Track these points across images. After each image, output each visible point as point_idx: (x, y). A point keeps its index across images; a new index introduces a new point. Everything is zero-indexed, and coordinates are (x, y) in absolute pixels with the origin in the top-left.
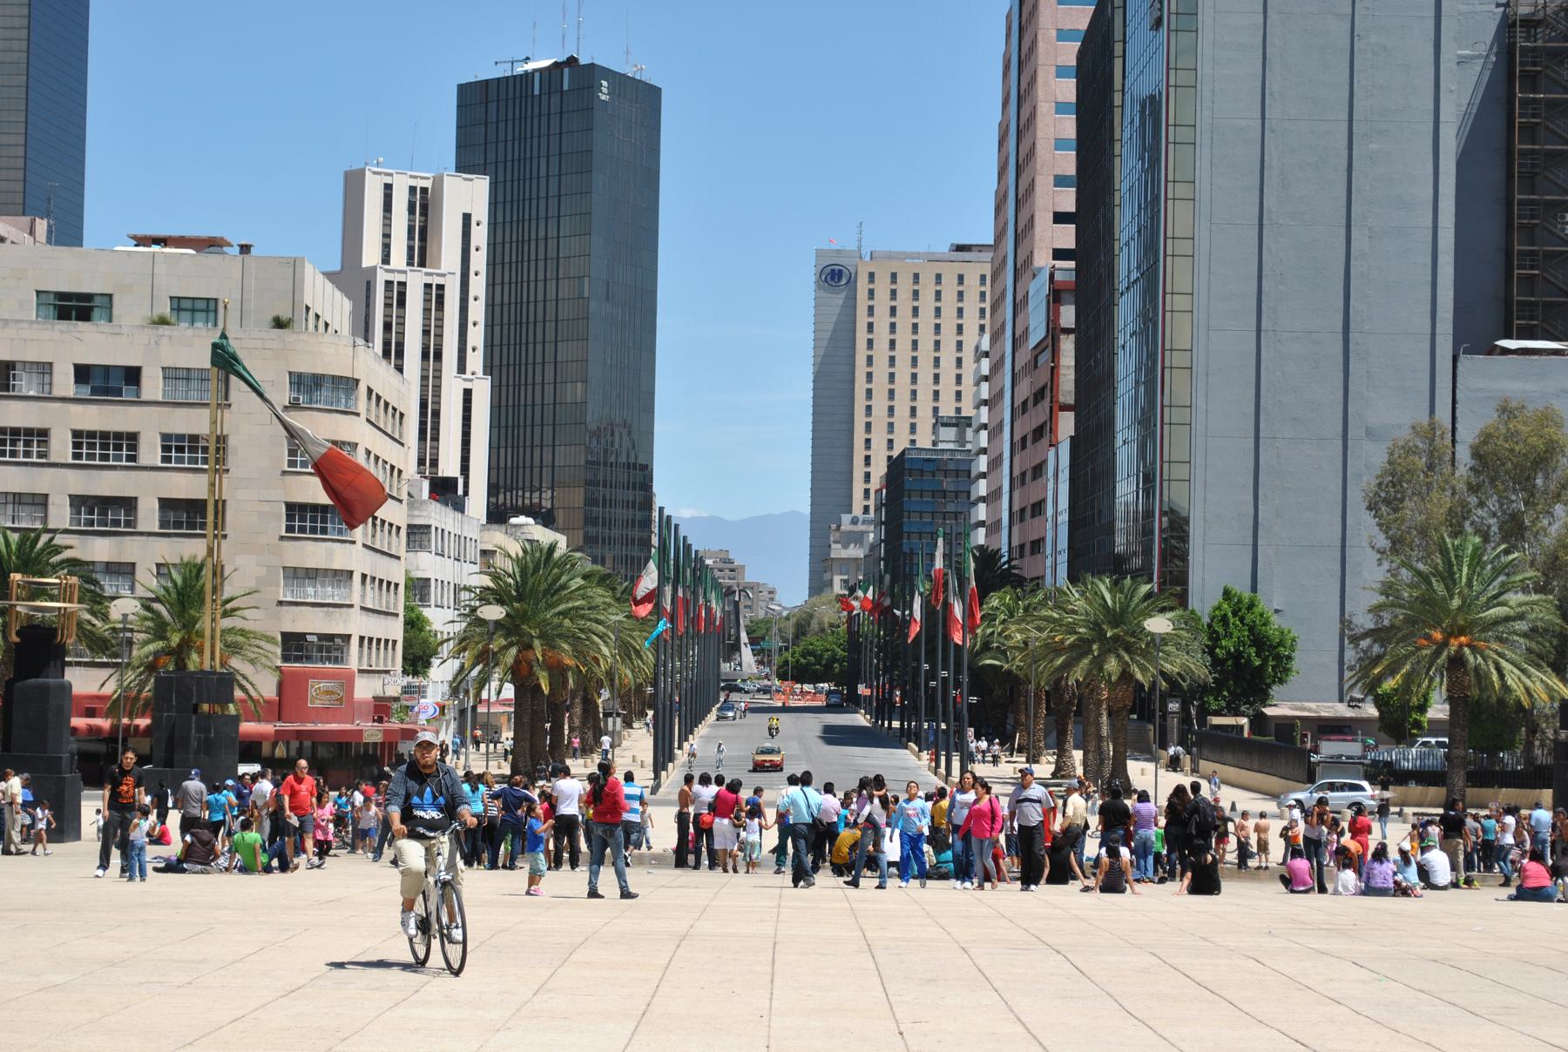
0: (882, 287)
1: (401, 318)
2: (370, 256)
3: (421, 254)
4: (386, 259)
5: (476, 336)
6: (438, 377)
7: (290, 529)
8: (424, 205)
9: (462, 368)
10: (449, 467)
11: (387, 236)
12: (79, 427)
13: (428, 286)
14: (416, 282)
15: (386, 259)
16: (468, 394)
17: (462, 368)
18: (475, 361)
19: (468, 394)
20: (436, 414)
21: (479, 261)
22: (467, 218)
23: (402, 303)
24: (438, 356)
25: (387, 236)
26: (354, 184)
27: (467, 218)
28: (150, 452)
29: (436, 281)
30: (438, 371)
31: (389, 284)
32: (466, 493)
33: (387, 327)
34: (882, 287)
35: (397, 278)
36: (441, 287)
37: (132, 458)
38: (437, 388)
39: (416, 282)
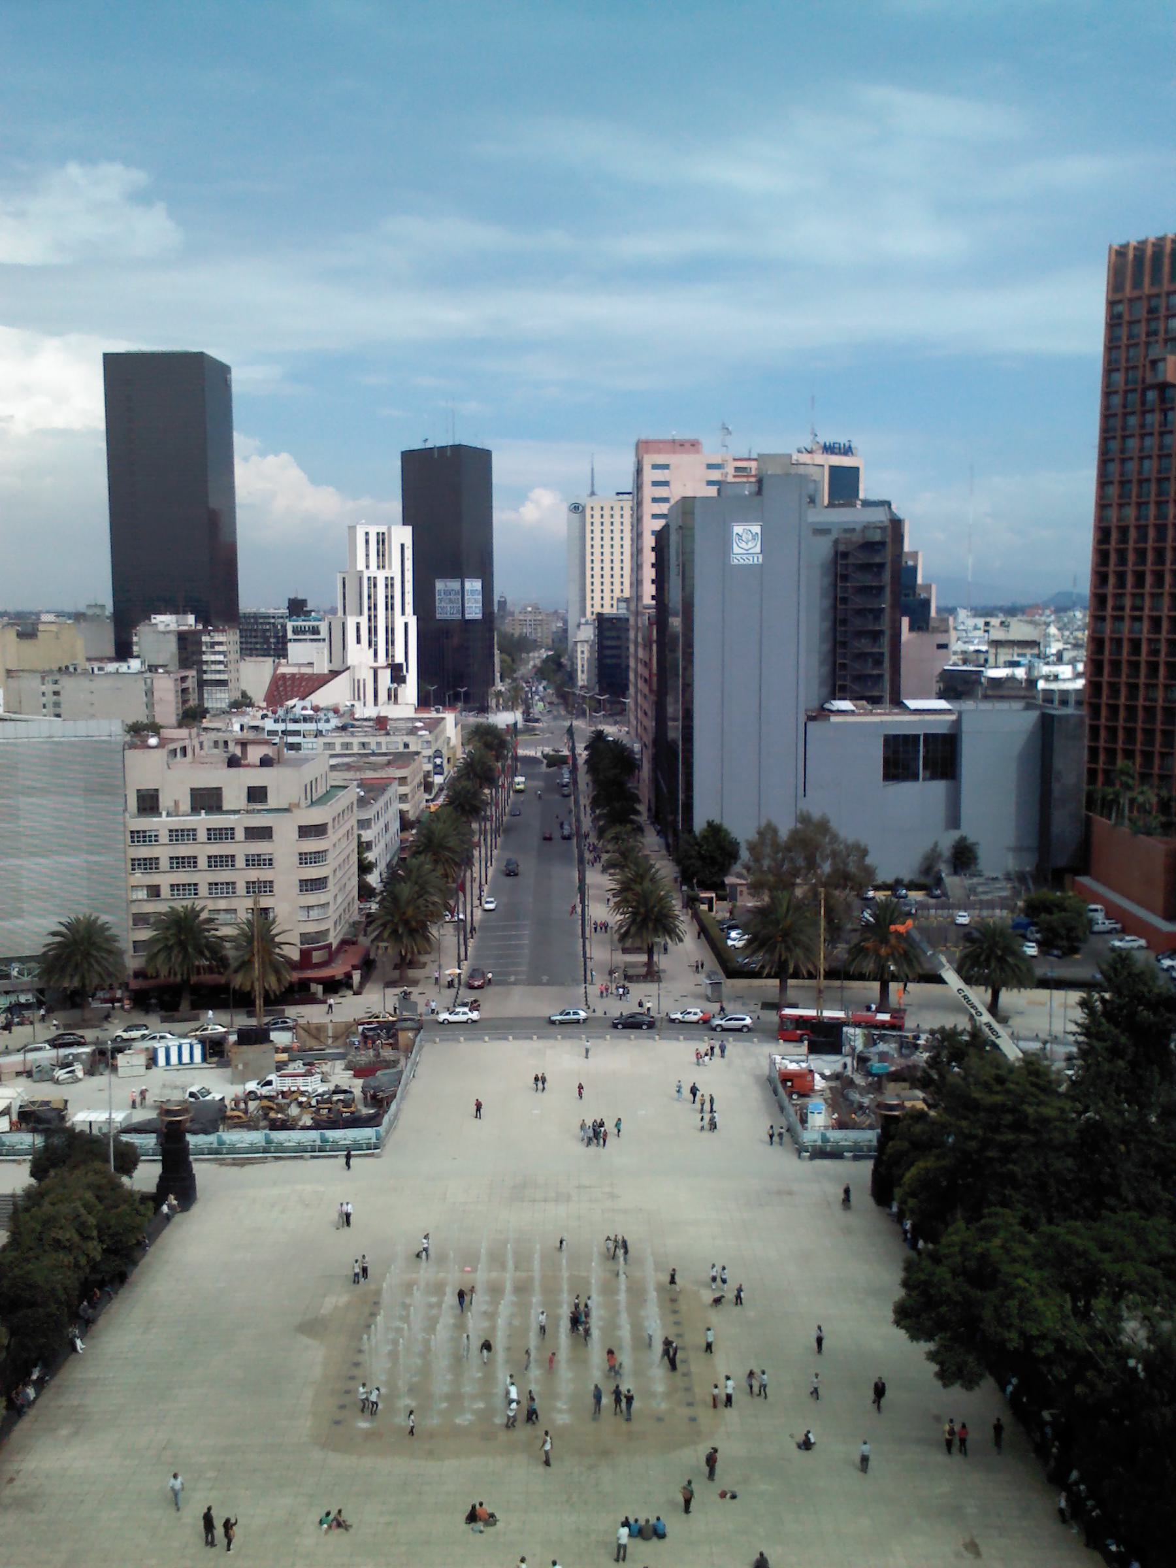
0: (597, 513)
1: (375, 592)
2: (361, 566)
3: (381, 566)
4: (367, 567)
5: (409, 598)
6: (393, 618)
7: (301, 891)
8: (382, 539)
9: (403, 613)
10: (399, 658)
11: (367, 555)
12: (210, 854)
13: (387, 578)
14: (381, 576)
15: (367, 567)
16: (406, 625)
17: (403, 613)
18: (409, 608)
19: (406, 625)
20: (393, 630)
21: (409, 565)
22: (402, 546)
23: (375, 586)
24: (392, 609)
25: (367, 555)
26: (352, 529)
27: (402, 546)
28: (240, 862)
29: (389, 575)
30: (393, 615)
31: (369, 578)
32: (407, 671)
33: (369, 597)
34: (597, 513)
35: (372, 575)
36: (392, 578)
37: (233, 866)
38: (393, 622)
39: (381, 576)
